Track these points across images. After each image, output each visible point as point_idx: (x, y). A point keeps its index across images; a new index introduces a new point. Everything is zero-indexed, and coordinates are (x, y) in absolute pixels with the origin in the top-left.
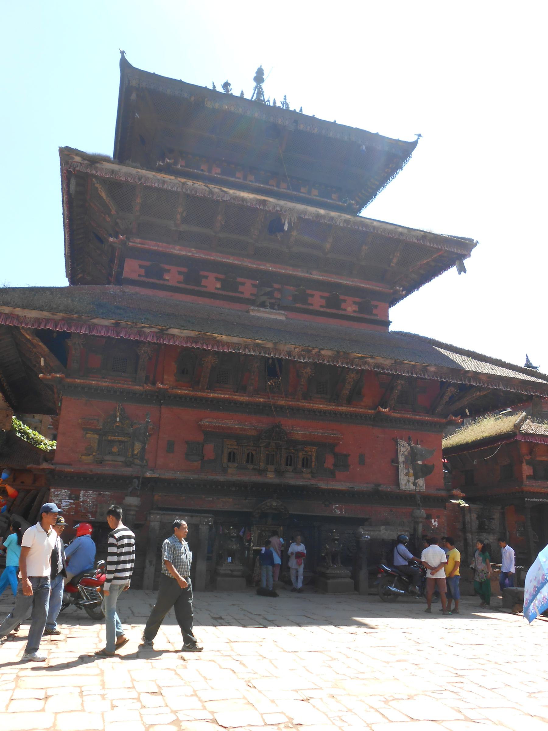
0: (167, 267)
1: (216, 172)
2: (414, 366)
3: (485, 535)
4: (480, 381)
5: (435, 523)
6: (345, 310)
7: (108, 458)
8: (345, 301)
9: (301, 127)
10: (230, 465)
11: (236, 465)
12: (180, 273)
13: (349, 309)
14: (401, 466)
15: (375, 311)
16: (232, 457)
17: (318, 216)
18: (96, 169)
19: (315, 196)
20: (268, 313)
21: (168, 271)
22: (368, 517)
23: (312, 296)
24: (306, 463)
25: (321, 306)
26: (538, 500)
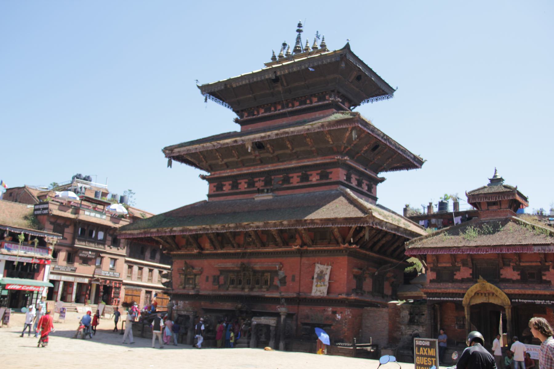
0: (224, 183)
1: (262, 113)
2: (275, 223)
3: (415, 327)
4: (317, 224)
5: (339, 317)
6: (311, 181)
7: (187, 286)
8: (311, 175)
9: (278, 74)
10: (230, 286)
11: (233, 286)
12: (230, 185)
13: (314, 179)
14: (315, 280)
15: (330, 176)
16: (232, 282)
17: (262, 137)
18: (174, 153)
19: (316, 102)
20: (263, 196)
21: (225, 185)
22: (293, 313)
23: (292, 177)
24: (266, 282)
25: (298, 183)
26: (439, 299)
